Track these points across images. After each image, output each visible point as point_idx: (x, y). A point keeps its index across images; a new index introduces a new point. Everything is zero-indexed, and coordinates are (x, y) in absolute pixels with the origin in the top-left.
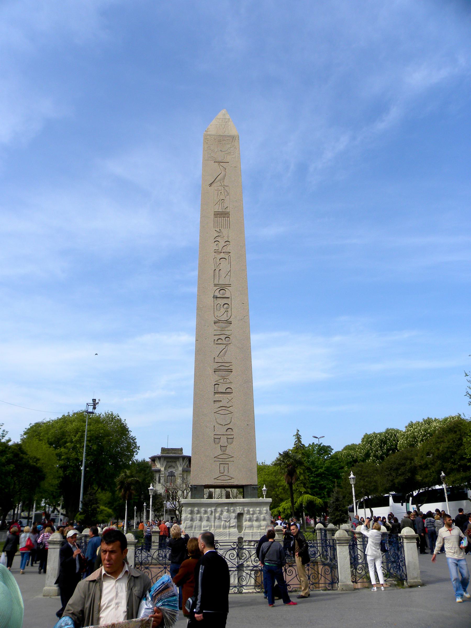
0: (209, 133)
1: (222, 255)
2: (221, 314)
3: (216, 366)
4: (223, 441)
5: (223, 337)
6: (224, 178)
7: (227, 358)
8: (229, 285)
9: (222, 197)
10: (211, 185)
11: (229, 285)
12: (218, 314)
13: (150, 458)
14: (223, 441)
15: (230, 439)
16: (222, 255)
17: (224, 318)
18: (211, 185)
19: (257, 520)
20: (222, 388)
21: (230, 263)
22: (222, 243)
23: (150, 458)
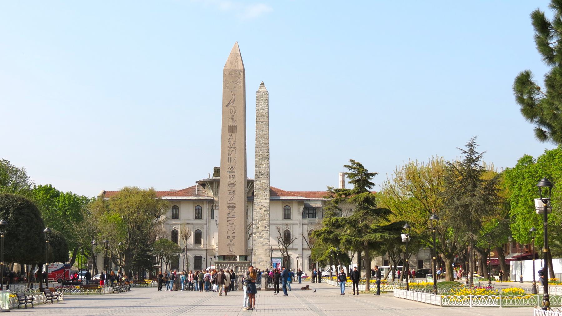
0: (226, 68)
1: (232, 149)
2: (231, 181)
3: (229, 205)
4: (231, 238)
5: (232, 192)
6: (234, 101)
7: (233, 201)
8: (235, 165)
9: (233, 114)
10: (227, 106)
11: (235, 165)
12: (230, 180)
13: (197, 182)
14: (231, 238)
15: (234, 238)
16: (232, 149)
17: (232, 182)
18: (227, 106)
19: (244, 269)
20: (231, 215)
21: (236, 153)
22: (232, 143)
23: (197, 182)
